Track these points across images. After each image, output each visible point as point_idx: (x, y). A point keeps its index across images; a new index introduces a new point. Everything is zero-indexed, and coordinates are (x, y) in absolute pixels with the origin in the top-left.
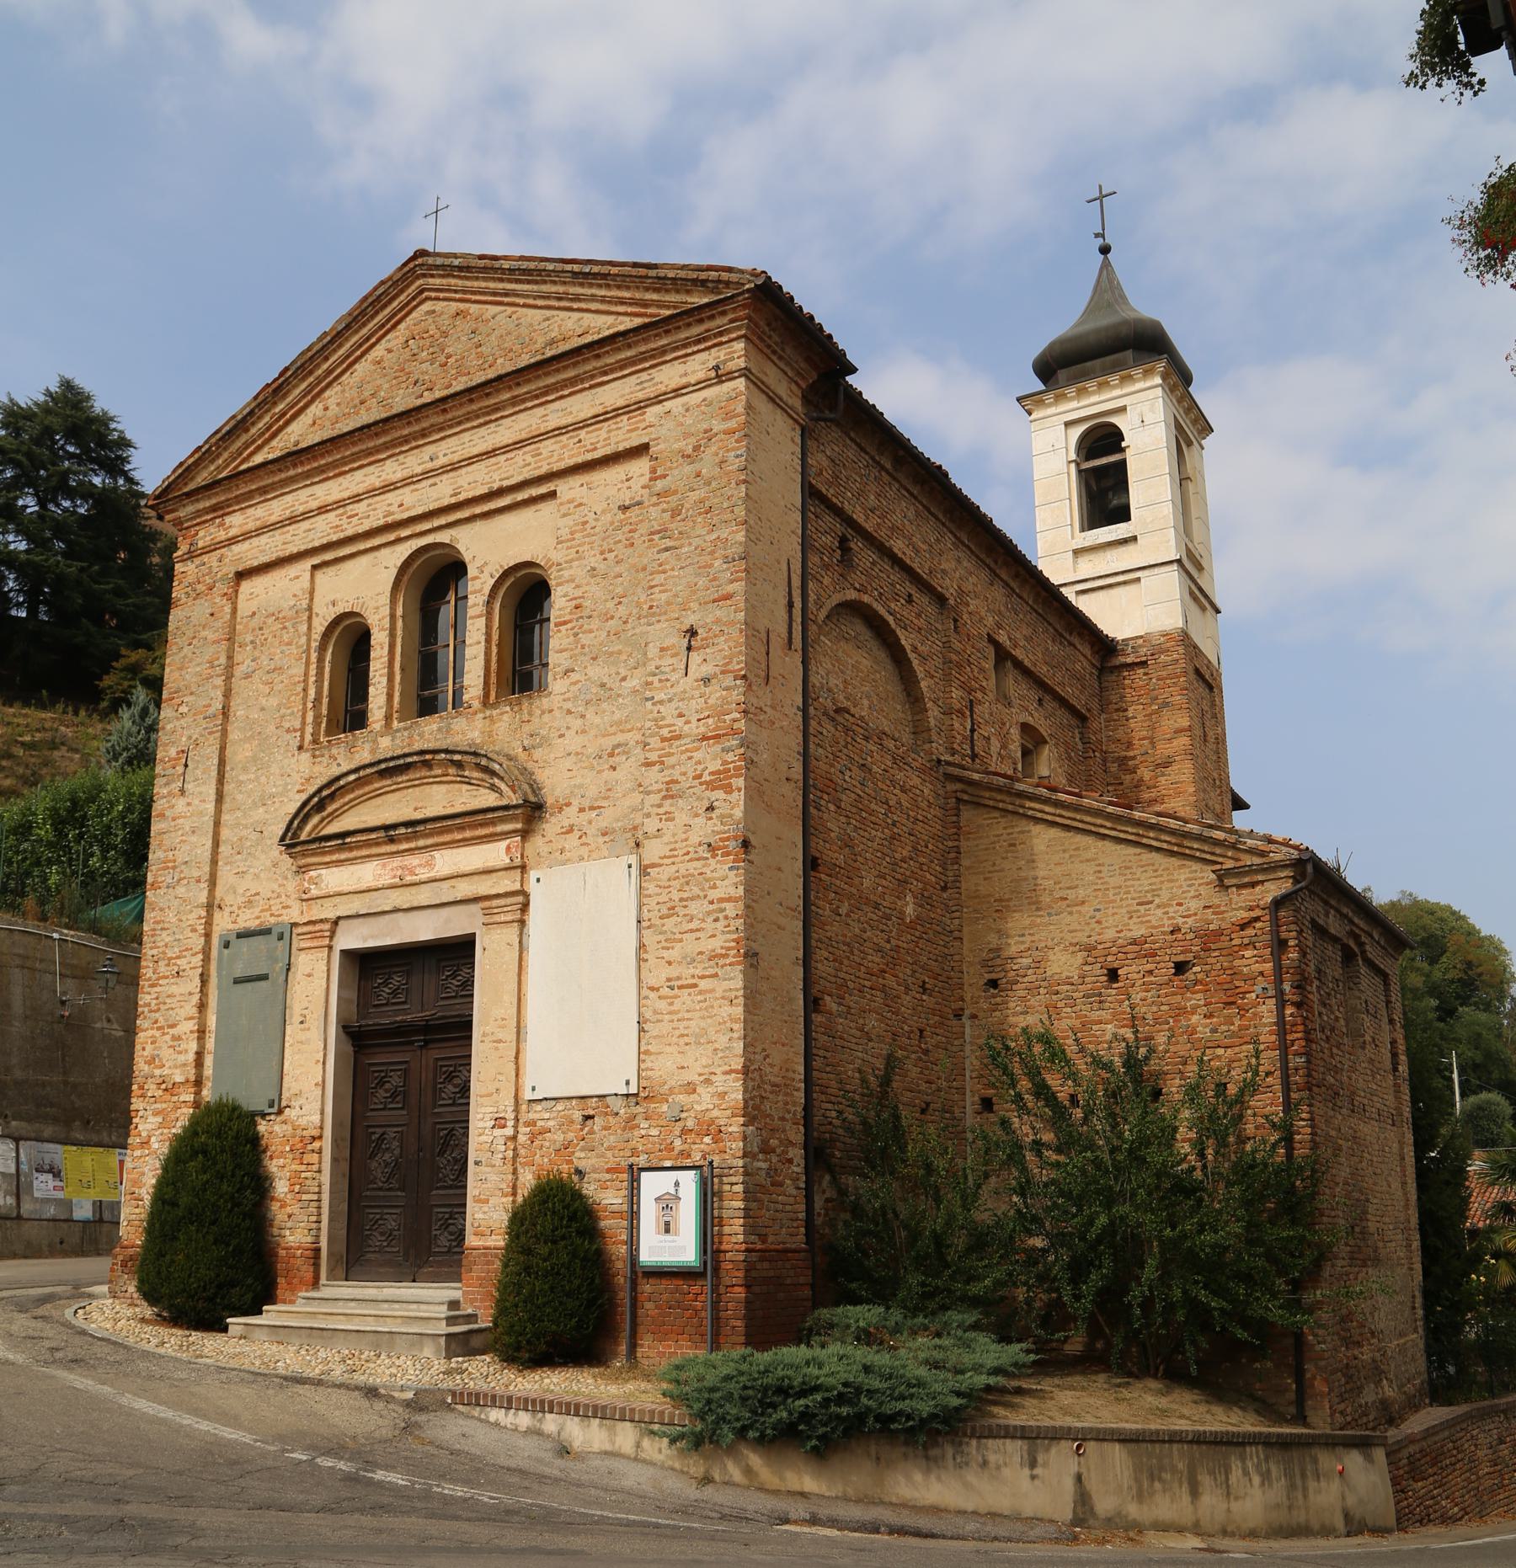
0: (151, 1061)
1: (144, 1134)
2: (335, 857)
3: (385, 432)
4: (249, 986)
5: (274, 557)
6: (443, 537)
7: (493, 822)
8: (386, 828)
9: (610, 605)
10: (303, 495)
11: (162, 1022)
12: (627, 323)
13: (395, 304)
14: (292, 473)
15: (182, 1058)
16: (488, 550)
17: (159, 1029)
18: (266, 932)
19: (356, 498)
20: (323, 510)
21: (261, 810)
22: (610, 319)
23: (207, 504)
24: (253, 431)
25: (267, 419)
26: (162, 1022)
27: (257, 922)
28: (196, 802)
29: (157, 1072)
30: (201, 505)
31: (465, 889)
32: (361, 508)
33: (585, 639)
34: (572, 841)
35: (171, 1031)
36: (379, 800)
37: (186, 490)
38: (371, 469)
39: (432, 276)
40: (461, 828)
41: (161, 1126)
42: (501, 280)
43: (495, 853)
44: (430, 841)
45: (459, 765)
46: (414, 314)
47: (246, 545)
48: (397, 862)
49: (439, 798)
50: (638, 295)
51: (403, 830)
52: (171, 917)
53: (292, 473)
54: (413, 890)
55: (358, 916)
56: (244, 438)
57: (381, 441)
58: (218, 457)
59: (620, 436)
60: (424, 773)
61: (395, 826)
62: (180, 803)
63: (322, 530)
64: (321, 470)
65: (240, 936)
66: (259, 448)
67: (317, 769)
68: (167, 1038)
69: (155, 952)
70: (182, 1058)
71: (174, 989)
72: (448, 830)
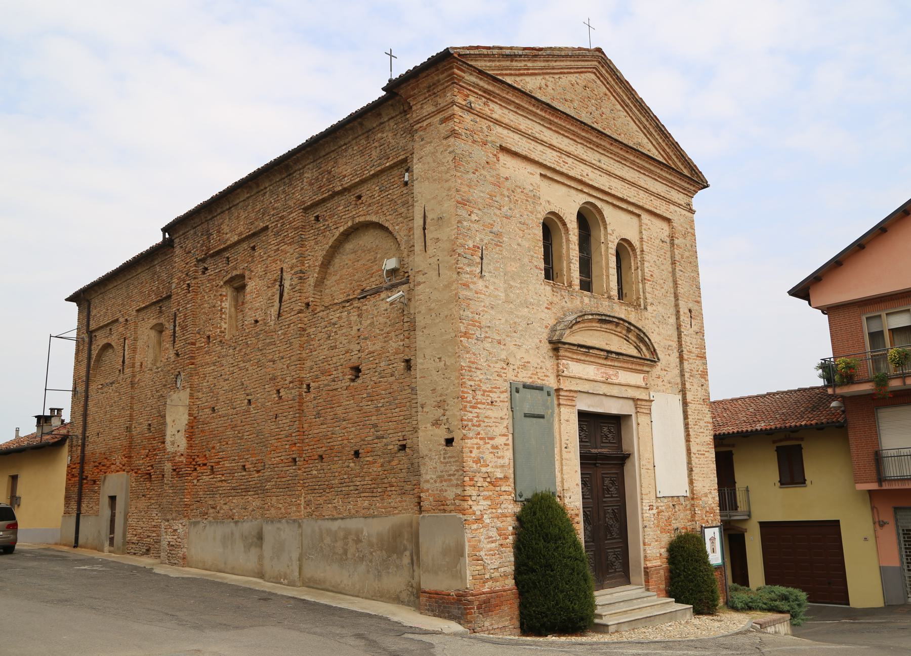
0: (477, 461)
1: (478, 513)
2: (579, 357)
3: (587, 132)
4: (534, 420)
5: (524, 153)
6: (599, 204)
7: (643, 365)
8: (609, 352)
9: (662, 282)
10: (538, 128)
11: (483, 435)
12: (661, 159)
13: (586, 63)
14: (538, 111)
15: (501, 461)
16: (618, 225)
17: (481, 439)
18: (540, 388)
19: (568, 155)
20: (551, 147)
21: (526, 310)
22: (657, 153)
23: (486, 86)
24: (514, 64)
25: (522, 64)
26: (483, 435)
27: (531, 380)
28: (492, 287)
29: (484, 469)
30: (481, 83)
31: (631, 393)
32: (570, 160)
33: (656, 292)
34: (659, 382)
35: (492, 442)
36: (591, 332)
37: (470, 63)
38: (572, 142)
39: (603, 67)
40: (633, 363)
41: (490, 507)
42: (629, 99)
43: (636, 379)
44: (619, 365)
45: (629, 330)
46: (588, 74)
47: (505, 132)
48: (603, 369)
49: (616, 344)
50: (671, 154)
51: (614, 355)
52: (482, 362)
53: (538, 111)
54: (611, 387)
55: (588, 393)
56: (508, 63)
57: (584, 134)
58: (493, 61)
59: (662, 208)
60: (613, 327)
61: (611, 352)
62: (481, 284)
63: (549, 157)
64: (550, 122)
65: (525, 386)
66: (511, 75)
67: (555, 299)
68: (489, 446)
69: (472, 383)
70: (501, 461)
71: (489, 413)
72: (627, 362)
